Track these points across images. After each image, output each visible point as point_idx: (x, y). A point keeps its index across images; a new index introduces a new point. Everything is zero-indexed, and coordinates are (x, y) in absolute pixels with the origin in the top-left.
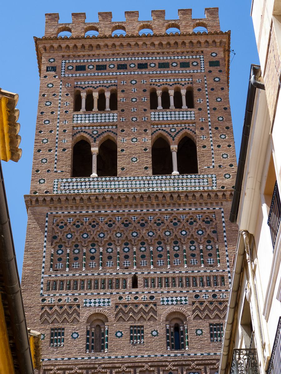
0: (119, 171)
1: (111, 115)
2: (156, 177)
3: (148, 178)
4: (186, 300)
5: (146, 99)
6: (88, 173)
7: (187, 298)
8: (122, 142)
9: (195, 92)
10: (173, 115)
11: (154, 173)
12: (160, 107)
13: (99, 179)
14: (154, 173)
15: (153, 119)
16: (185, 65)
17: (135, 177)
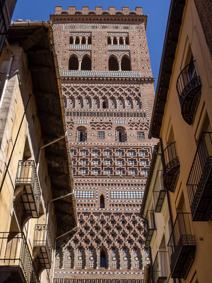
0: (92, 68)
1: (88, 46)
2: (110, 72)
3: (106, 72)
4: (124, 122)
5: (106, 41)
6: (77, 68)
7: (125, 121)
8: (94, 56)
9: (130, 39)
10: (118, 47)
11: (109, 70)
12: (112, 44)
13: (82, 71)
14: (109, 70)
15: (109, 48)
16: (125, 28)
17: (100, 70)
